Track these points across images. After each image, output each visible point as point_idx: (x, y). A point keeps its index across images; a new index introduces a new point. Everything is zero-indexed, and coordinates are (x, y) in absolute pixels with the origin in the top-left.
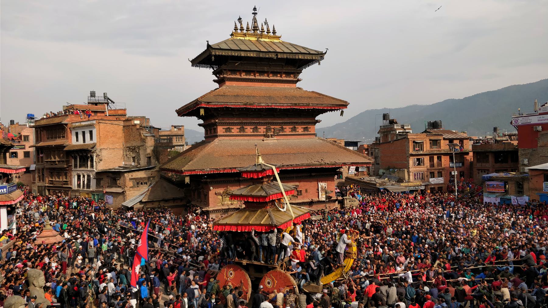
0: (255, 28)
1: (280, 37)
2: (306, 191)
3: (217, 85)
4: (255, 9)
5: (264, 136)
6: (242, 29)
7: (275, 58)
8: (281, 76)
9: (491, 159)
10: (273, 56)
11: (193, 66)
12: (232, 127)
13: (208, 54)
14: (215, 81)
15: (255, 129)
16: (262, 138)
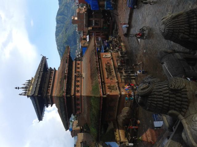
0: (26, 88)
1: (32, 78)
2: (108, 61)
3: (54, 105)
4: (16, 88)
5: (81, 78)
6: (25, 93)
7: (43, 72)
8: (52, 75)
9: (91, 19)
10: (41, 73)
11: (42, 120)
12: (77, 90)
13: (36, 98)
14: (52, 106)
15: (78, 81)
16: (82, 79)
